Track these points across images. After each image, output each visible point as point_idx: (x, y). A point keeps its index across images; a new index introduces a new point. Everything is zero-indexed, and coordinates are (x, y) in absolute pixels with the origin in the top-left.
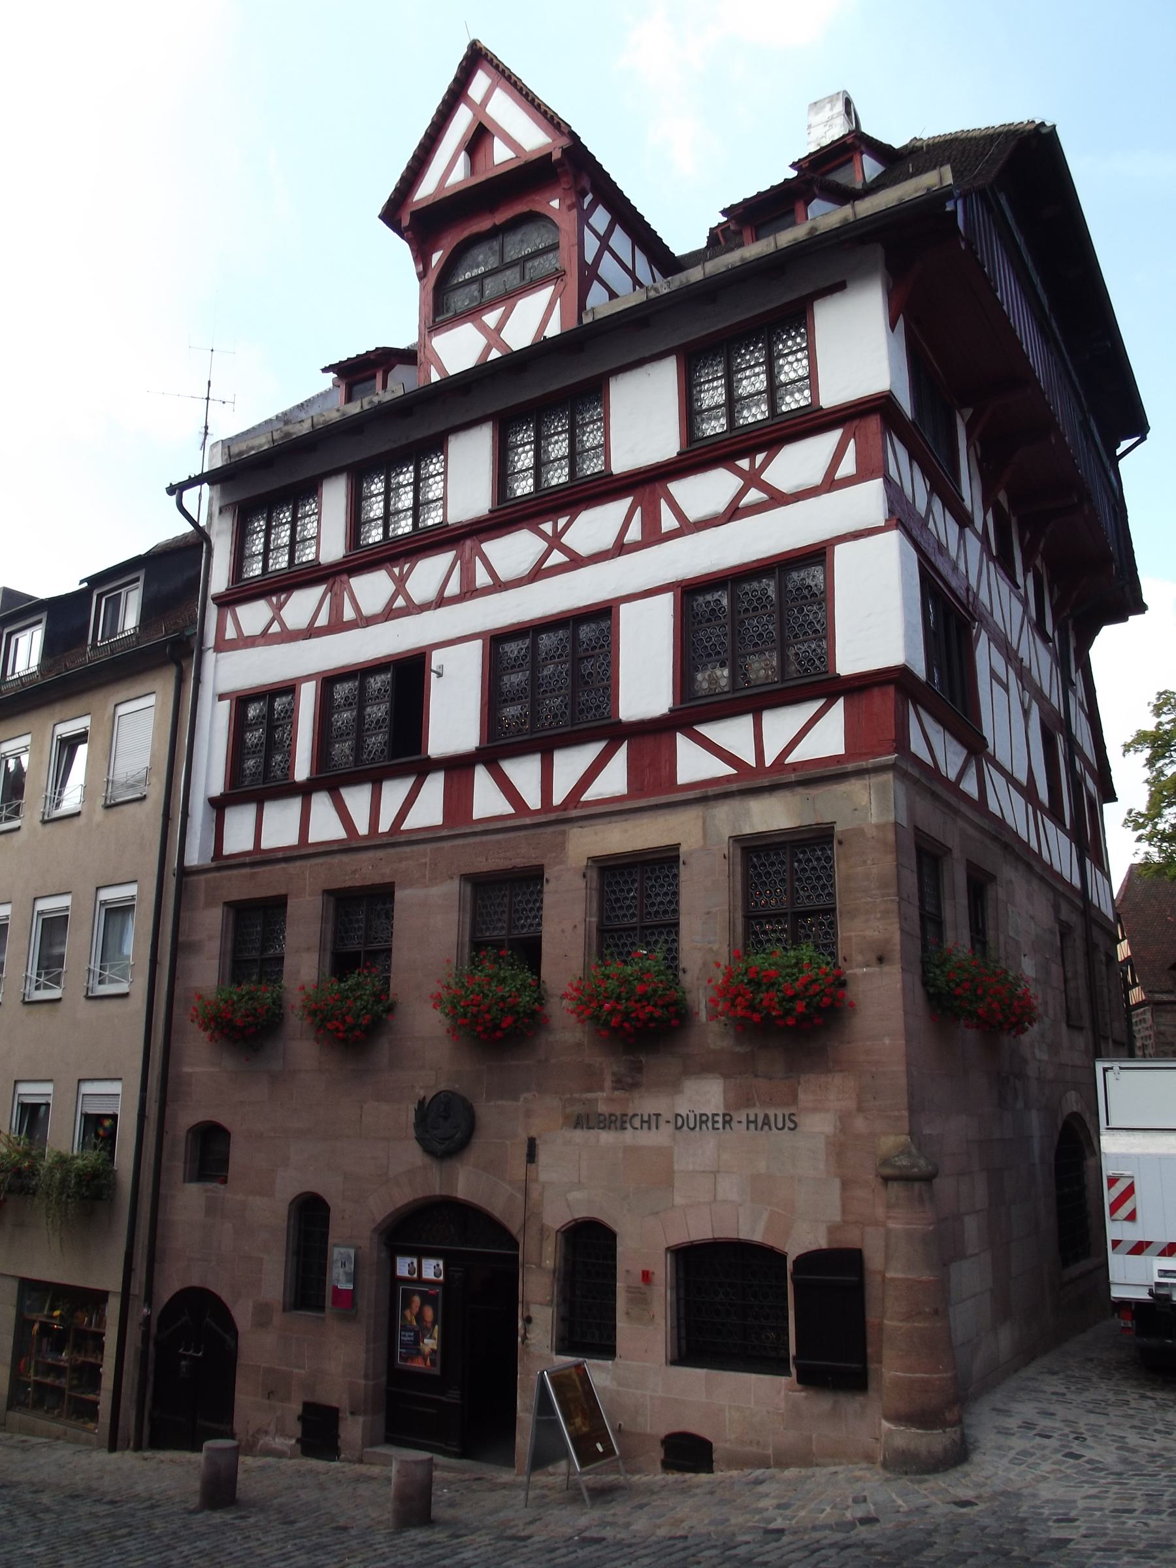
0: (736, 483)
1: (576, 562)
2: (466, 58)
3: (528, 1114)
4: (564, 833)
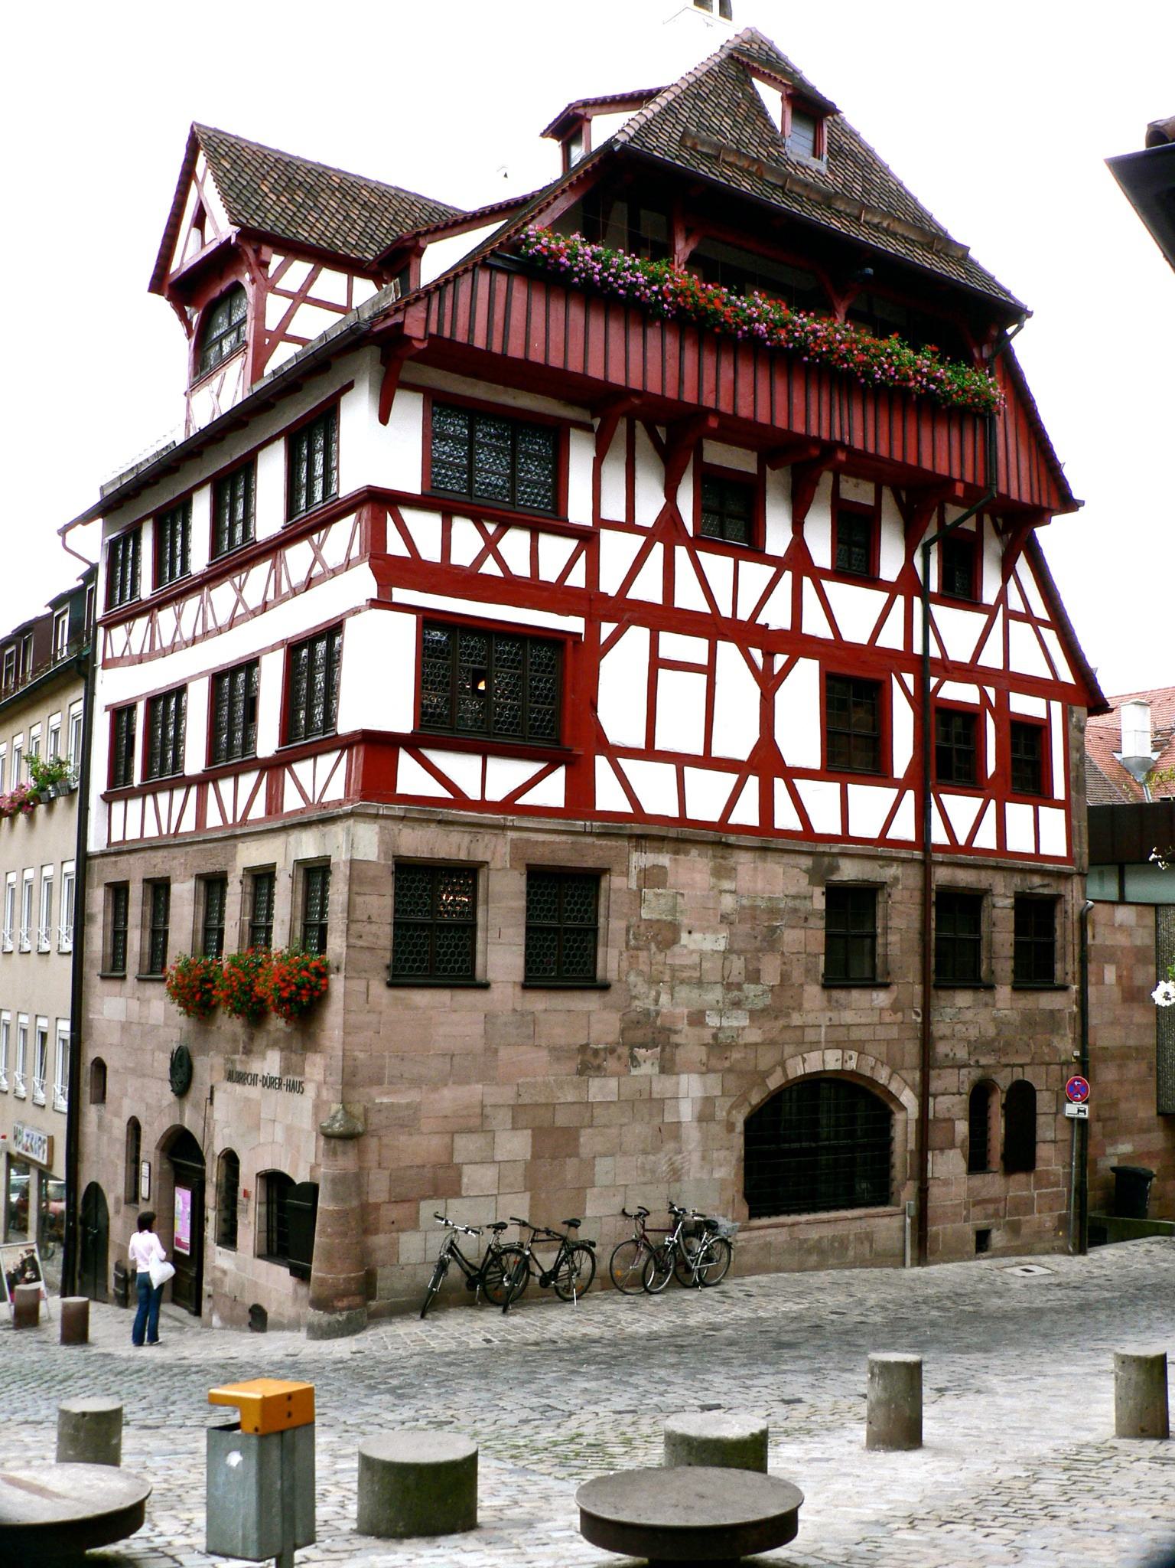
2: (190, 138)
4: (235, 846)
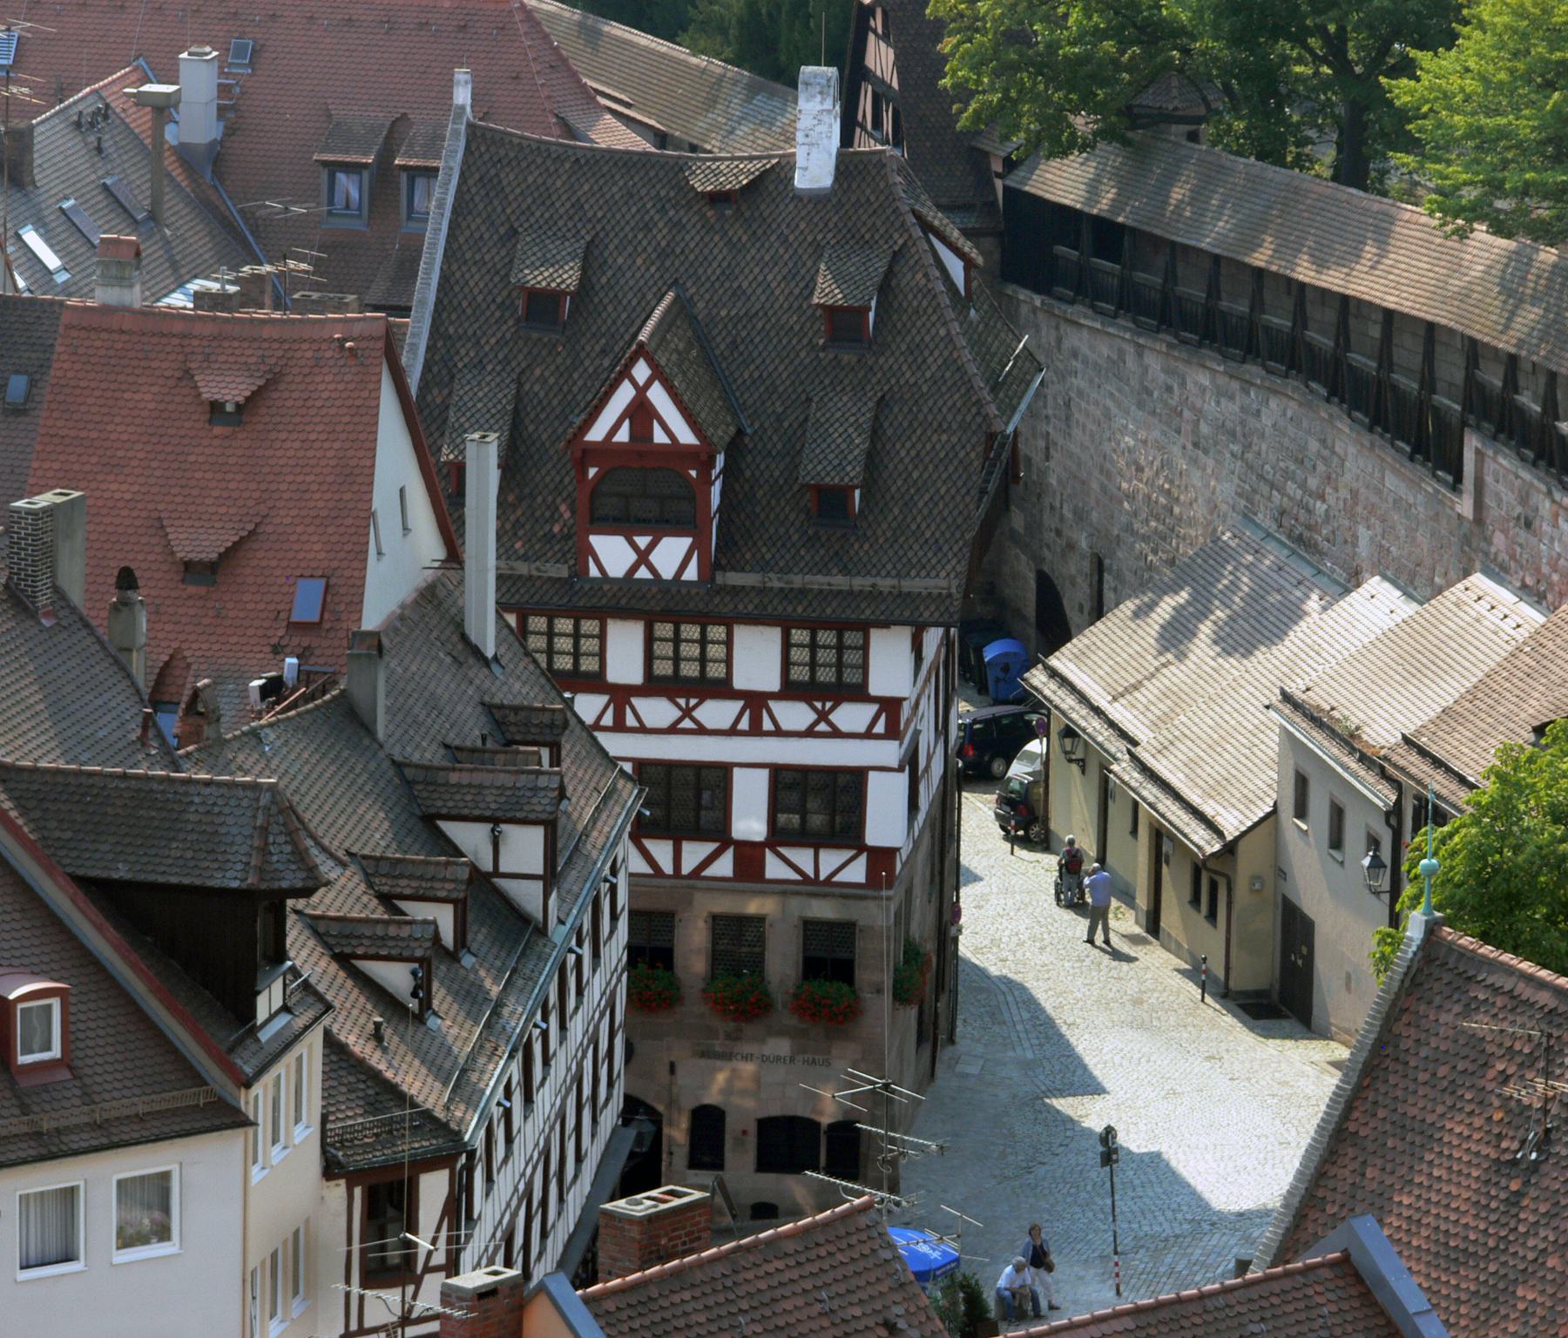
0: (813, 716)
1: (701, 730)
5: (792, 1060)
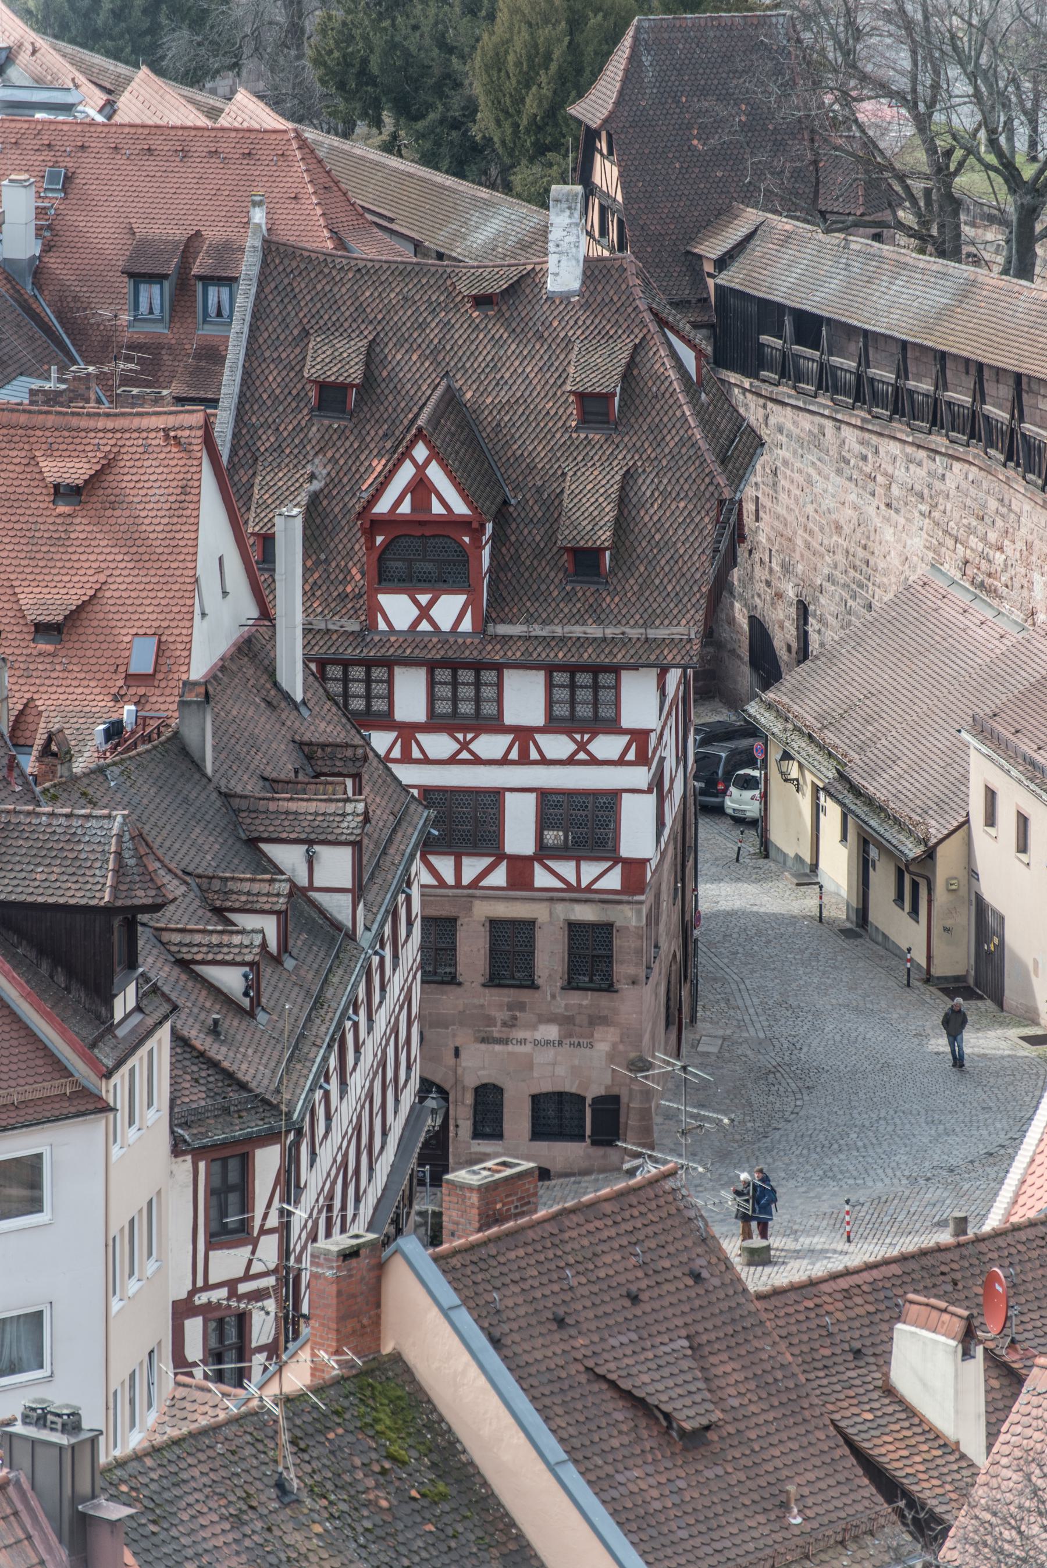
0: (573, 747)
3: (454, 1036)
5: (560, 1043)
